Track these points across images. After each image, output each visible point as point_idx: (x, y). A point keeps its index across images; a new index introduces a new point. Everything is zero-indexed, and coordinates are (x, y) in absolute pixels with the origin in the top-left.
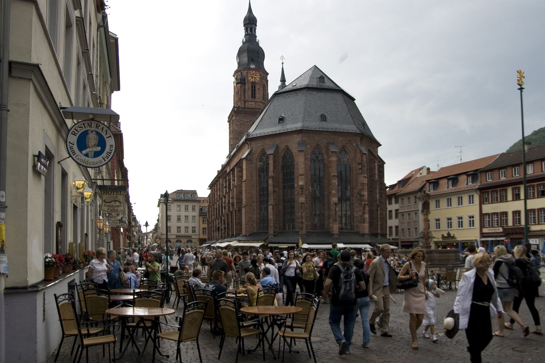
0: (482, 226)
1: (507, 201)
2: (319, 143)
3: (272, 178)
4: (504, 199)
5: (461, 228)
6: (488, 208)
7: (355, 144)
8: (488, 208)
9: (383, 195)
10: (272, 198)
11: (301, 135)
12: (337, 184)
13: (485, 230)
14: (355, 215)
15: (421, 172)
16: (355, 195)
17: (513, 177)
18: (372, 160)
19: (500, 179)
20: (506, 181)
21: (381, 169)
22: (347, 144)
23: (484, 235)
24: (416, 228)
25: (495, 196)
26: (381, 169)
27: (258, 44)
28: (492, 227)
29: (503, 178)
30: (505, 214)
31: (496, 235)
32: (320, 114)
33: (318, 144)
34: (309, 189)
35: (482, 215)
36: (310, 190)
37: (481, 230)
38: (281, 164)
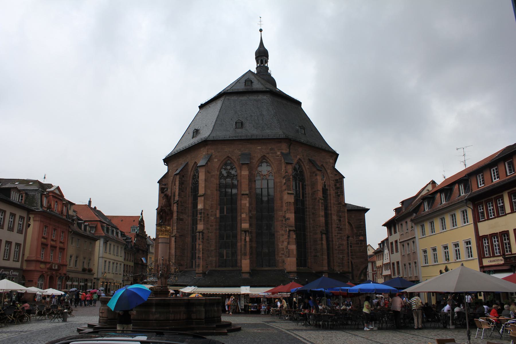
0: (481, 256)
1: (506, 215)
2: (230, 155)
3: (177, 202)
4: (500, 212)
5: (471, 258)
6: (487, 228)
7: (279, 153)
8: (487, 228)
9: (342, 219)
10: (176, 228)
11: (206, 148)
12: (248, 205)
13: (486, 262)
14: (280, 246)
15: (426, 188)
16: (280, 219)
17: (507, 176)
18: (314, 172)
19: (492, 181)
20: (499, 183)
21: (338, 185)
22: (268, 153)
23: (486, 269)
24: (415, 263)
25: (491, 208)
26: (338, 185)
27: (270, 75)
28: (494, 256)
29: (497, 179)
30: (506, 233)
31: (495, 268)
32: (243, 120)
33: (228, 157)
34: (216, 215)
35: (480, 239)
36: (218, 215)
37: (481, 262)
38: (190, 185)
